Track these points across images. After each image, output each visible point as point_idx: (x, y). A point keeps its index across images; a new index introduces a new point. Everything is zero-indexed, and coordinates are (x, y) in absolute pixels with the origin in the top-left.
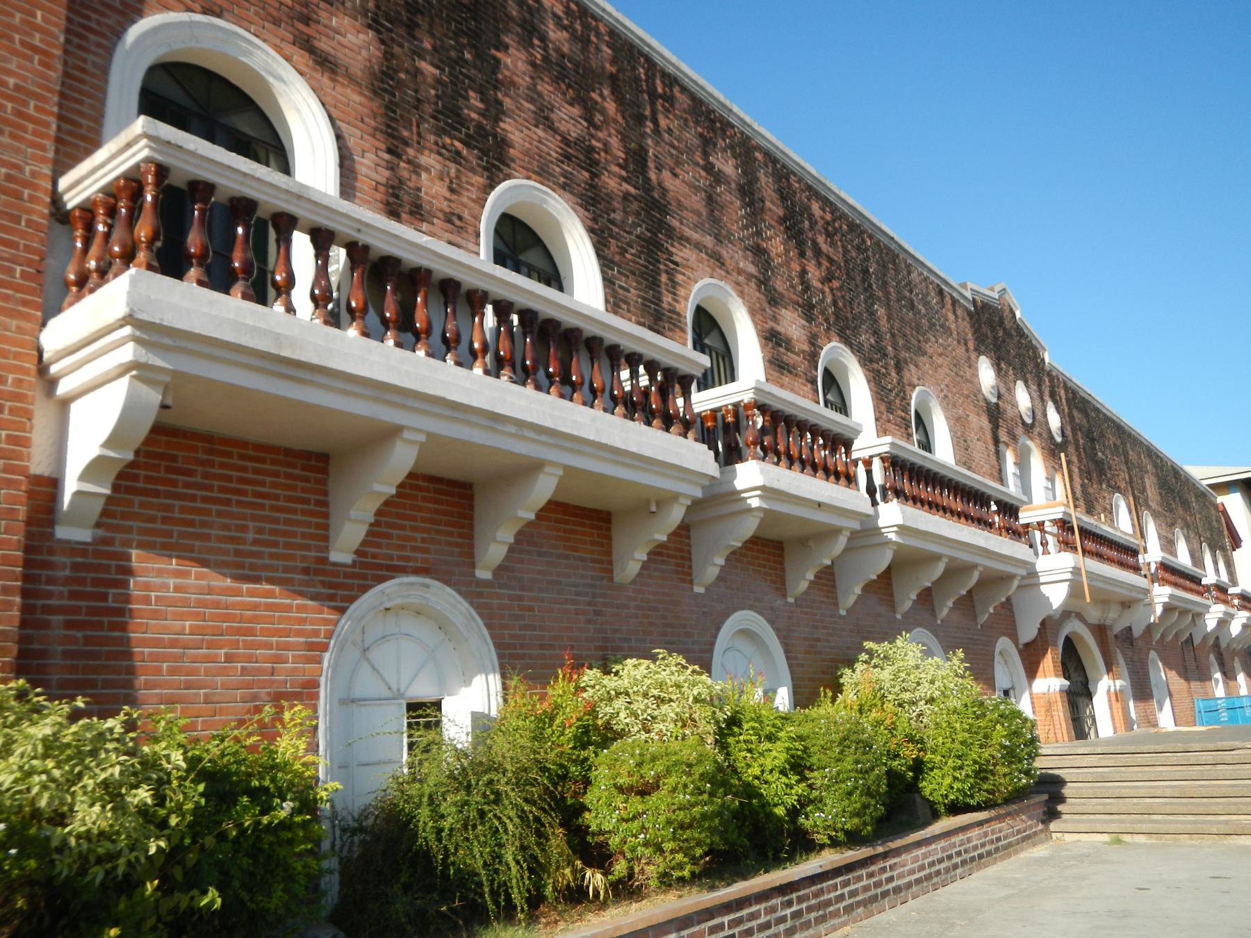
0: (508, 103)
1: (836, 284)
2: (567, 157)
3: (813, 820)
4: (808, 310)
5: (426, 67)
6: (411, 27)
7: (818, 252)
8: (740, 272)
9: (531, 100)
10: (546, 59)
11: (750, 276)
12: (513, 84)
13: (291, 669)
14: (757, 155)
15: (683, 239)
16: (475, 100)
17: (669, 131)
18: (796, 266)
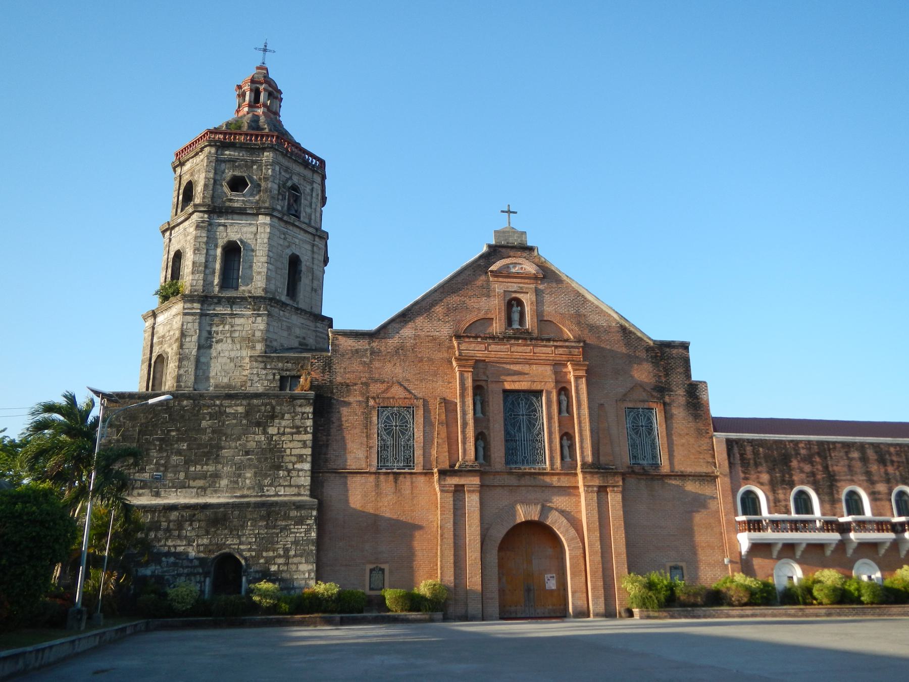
0: (793, 472)
1: (901, 468)
2: (808, 477)
3: (862, 598)
4: (888, 481)
5: (778, 475)
6: (774, 469)
7: (892, 462)
8: (860, 481)
9: (798, 469)
10: (801, 459)
11: (863, 480)
12: (794, 468)
13: (770, 572)
14: (867, 446)
15: (840, 481)
16: (787, 476)
17: (835, 456)
18: (882, 470)
